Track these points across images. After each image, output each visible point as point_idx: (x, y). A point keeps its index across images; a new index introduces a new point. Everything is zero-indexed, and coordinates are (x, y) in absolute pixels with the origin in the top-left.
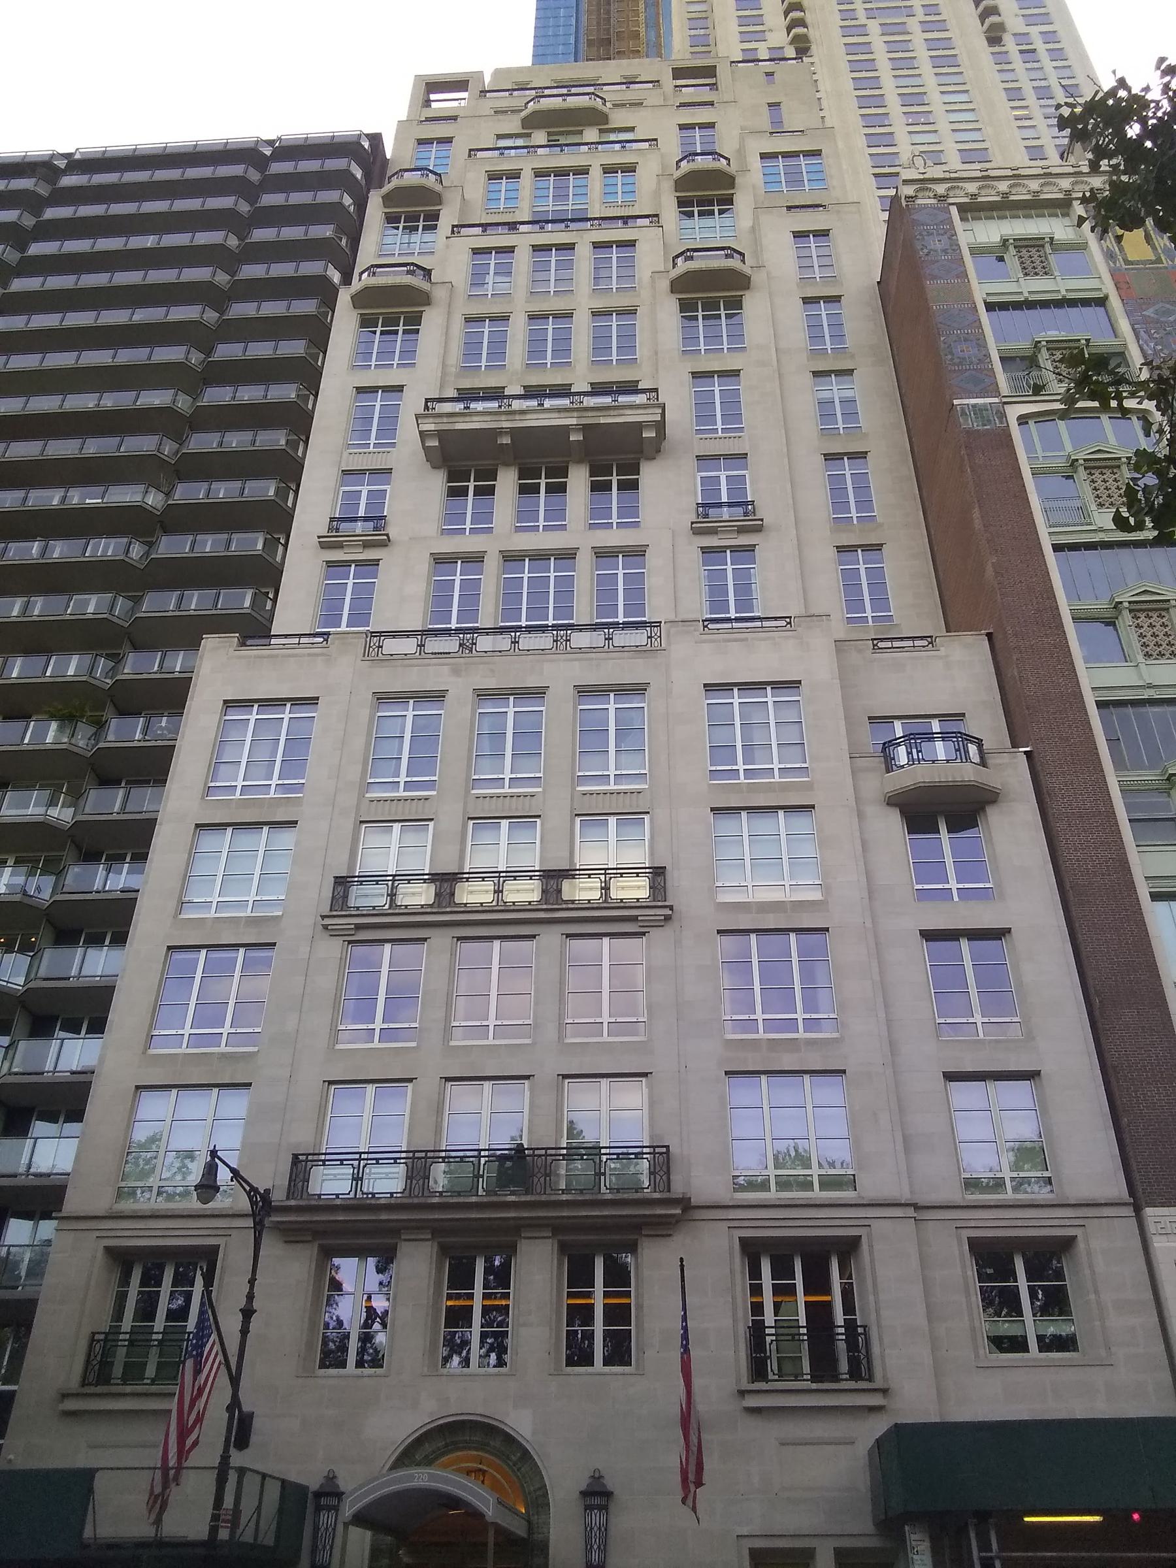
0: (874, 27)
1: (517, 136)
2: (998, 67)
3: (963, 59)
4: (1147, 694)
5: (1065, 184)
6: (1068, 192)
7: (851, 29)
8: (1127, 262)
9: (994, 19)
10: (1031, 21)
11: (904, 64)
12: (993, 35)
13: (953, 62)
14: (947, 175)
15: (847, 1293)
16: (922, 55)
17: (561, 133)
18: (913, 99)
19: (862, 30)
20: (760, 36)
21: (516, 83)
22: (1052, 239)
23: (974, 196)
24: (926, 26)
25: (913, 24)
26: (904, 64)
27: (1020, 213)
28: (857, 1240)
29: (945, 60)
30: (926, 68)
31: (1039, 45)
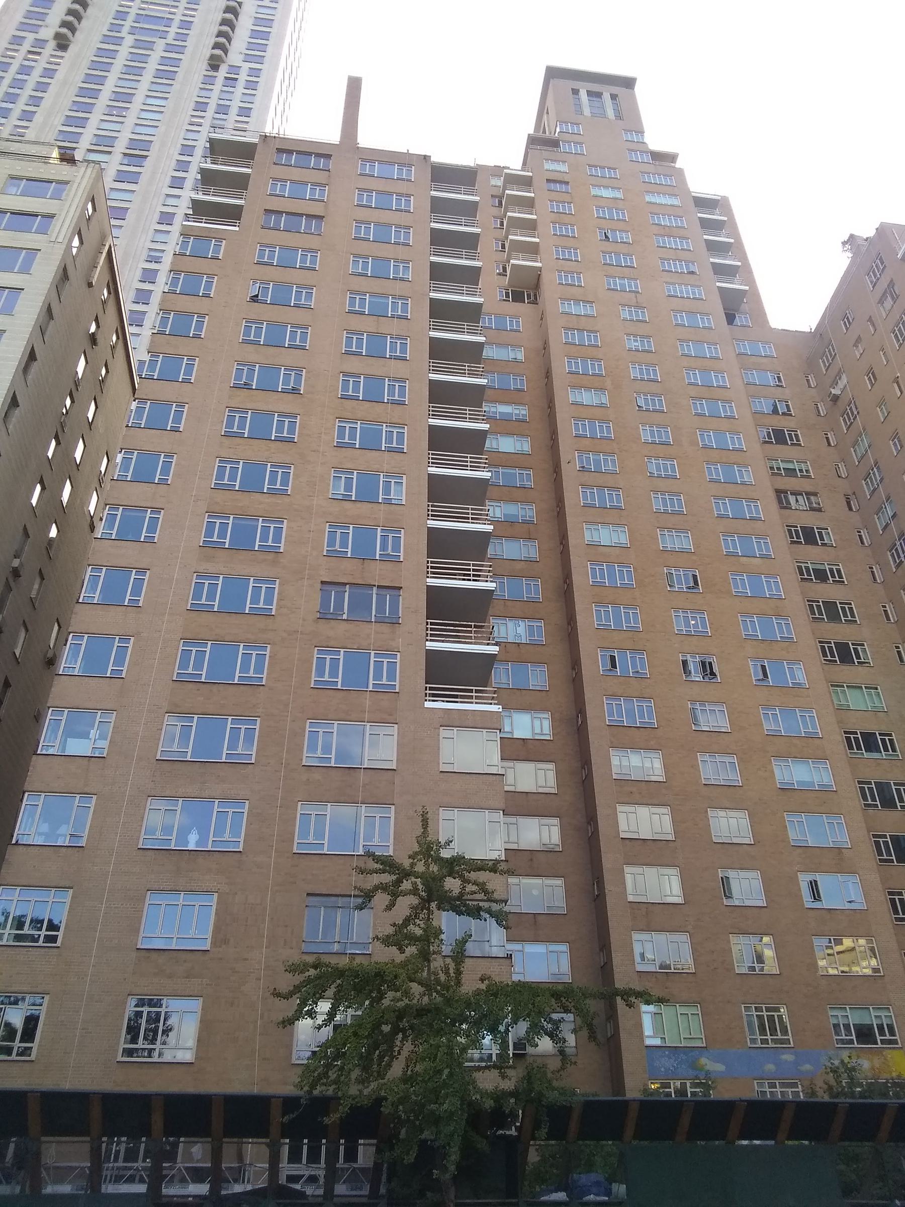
0: (129, 40)
3: (179, 77)
7: (113, 38)
10: (248, 59)
11: (133, 71)
12: (213, 63)
13: (171, 76)
16: (152, 65)
18: (123, 97)
19: (118, 41)
20: (35, 29)
24: (169, 48)
25: (160, 44)
26: (133, 71)
29: (166, 74)
30: (147, 77)
31: (243, 77)
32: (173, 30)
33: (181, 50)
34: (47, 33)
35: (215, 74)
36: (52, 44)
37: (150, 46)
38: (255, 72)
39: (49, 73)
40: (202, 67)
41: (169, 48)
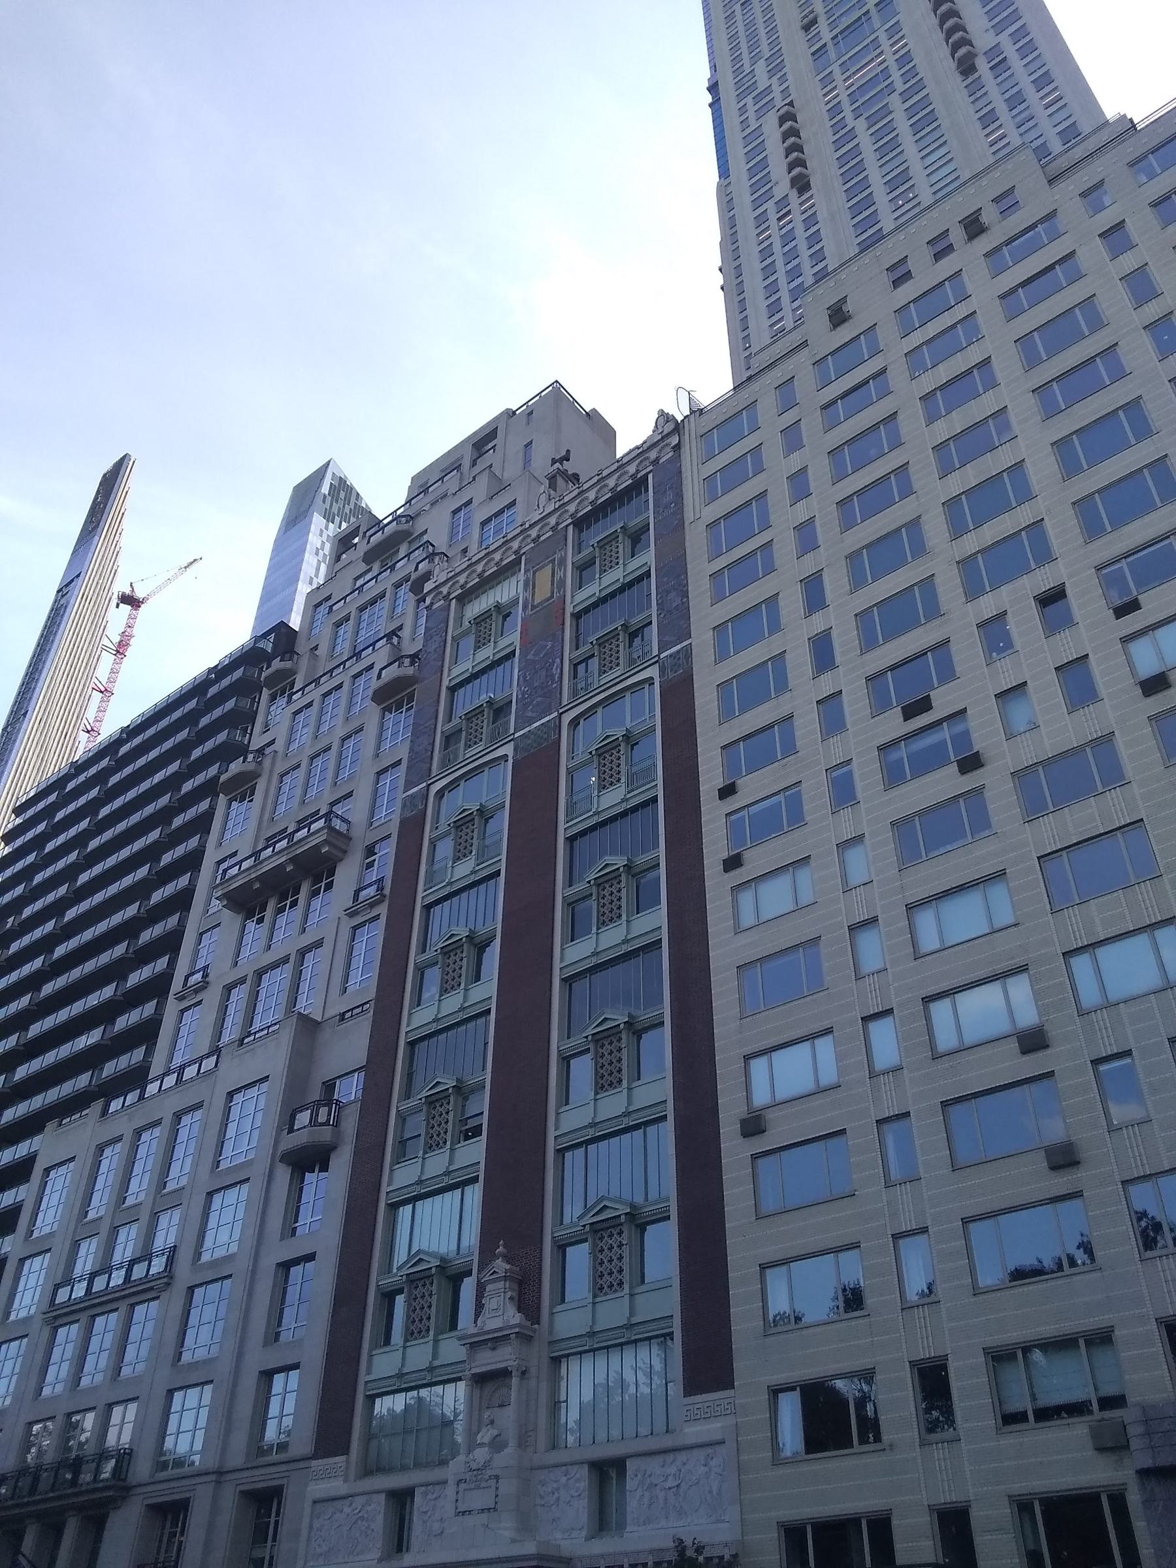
0: (861, 125)
1: (366, 573)
2: (972, 98)
3: (941, 111)
4: (434, 1027)
5: (515, 545)
6: (516, 552)
7: (844, 137)
8: (533, 607)
9: (962, 51)
11: (888, 147)
13: (932, 117)
14: (451, 575)
15: (277, 1522)
16: (903, 126)
17: (387, 558)
18: (899, 181)
19: (852, 134)
20: (768, 196)
21: (442, 471)
22: (498, 607)
23: (462, 587)
26: (888, 147)
27: (487, 587)
28: (187, 1500)
29: (925, 120)
32: (896, 75)
33: (920, 85)
34: (782, 186)
35: (976, 75)
36: (793, 194)
37: (886, 111)
38: (1023, 32)
39: (811, 221)
40: (956, 82)
41: (905, 96)
